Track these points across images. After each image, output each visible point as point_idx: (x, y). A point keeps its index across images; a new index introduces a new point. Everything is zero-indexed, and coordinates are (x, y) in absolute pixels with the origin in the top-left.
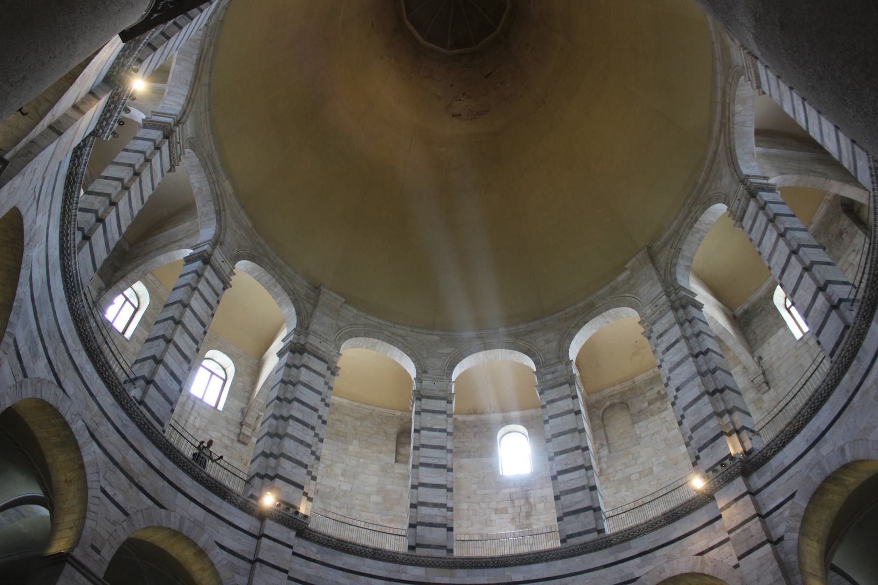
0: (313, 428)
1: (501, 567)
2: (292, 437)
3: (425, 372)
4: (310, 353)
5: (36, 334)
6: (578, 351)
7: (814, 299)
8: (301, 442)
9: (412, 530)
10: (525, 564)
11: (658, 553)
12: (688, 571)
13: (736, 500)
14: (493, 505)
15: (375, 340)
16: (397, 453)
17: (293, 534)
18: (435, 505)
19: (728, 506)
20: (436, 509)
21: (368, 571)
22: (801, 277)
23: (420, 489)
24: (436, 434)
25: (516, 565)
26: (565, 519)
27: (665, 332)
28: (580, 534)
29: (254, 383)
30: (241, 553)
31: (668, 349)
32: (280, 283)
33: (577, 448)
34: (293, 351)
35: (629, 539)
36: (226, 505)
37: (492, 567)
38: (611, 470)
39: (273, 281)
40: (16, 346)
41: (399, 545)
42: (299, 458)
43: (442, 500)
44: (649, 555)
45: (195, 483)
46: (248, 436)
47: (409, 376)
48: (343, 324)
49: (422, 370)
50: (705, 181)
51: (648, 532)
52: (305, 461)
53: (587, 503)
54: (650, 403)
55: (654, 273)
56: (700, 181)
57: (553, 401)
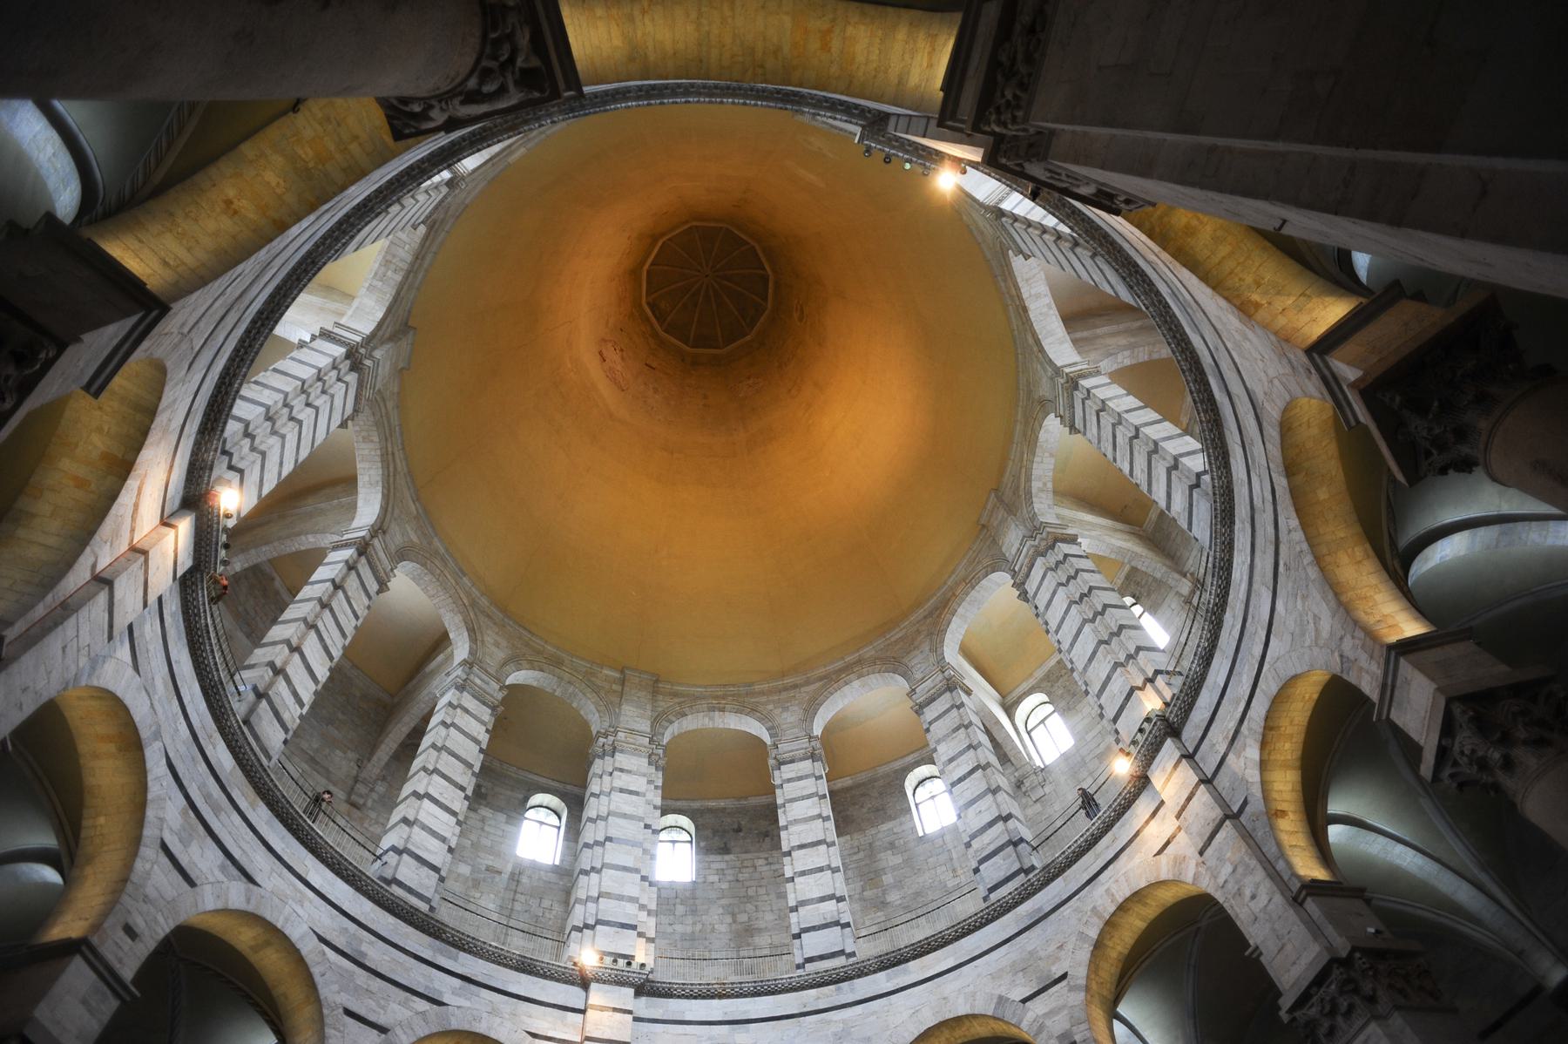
7: (823, 899)
8: (281, 464)
10: (333, 870)
11: (485, 993)
13: (615, 1010)
15: (376, 439)
18: (295, 694)
19: (602, 1009)
21: (186, 701)
22: (821, 869)
24: (349, 611)
25: (323, 861)
27: (629, 772)
28: (410, 890)
31: (622, 791)
38: (373, 815)
39: (405, 266)
44: (473, 987)
49: (378, 529)
50: (762, 693)
51: (488, 960)
55: (649, 707)
56: (757, 688)
57: (466, 711)
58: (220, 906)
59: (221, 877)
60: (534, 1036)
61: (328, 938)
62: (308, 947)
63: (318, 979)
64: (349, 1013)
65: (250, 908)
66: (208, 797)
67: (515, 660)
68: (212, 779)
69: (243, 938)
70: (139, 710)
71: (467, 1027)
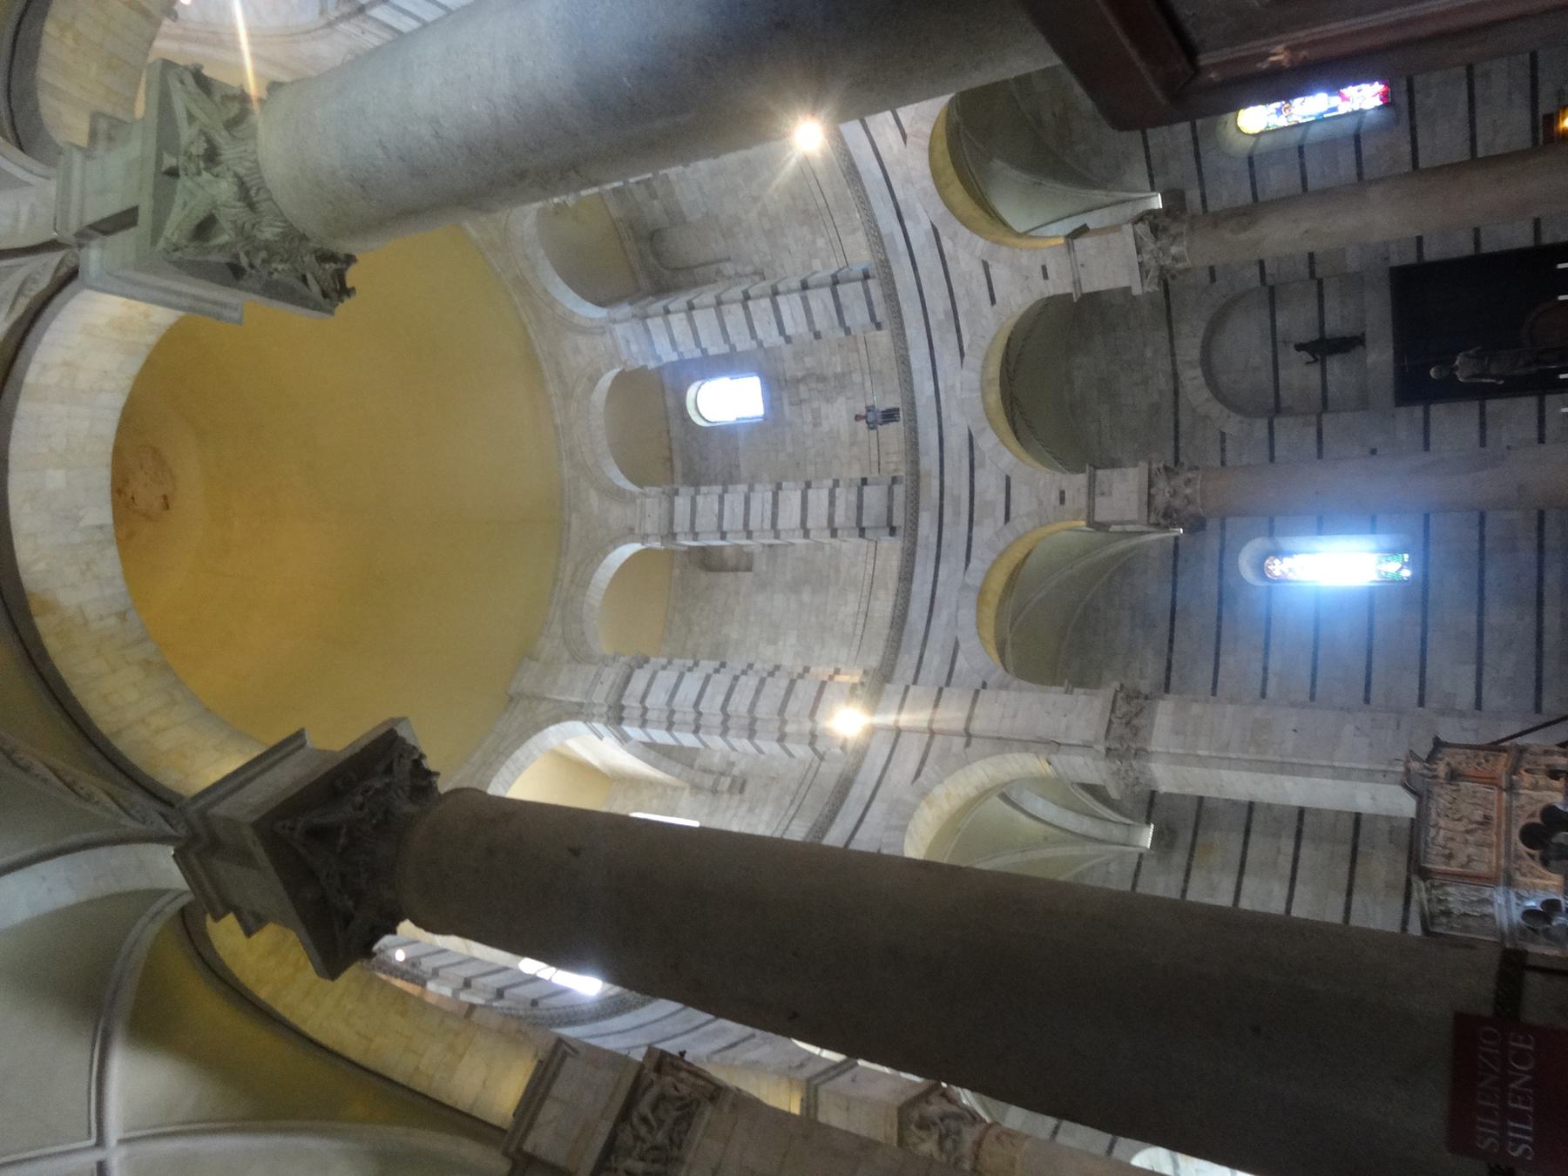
0: (736, 678)
2: (753, 705)
3: (631, 530)
4: (621, 696)
5: (694, 1034)
6: (589, 304)
8: (758, 692)
9: (868, 533)
11: (899, 195)
12: (926, 155)
14: (807, 429)
16: (736, 569)
17: (888, 686)
20: (838, 502)
21: (930, 587)
23: (810, 525)
26: (848, 323)
28: (870, 304)
29: (651, 783)
30: (923, 748)
32: (512, 753)
33: (746, 308)
34: (620, 720)
35: (879, 237)
36: (861, 777)
38: (756, 259)
39: (509, 763)
40: (719, 1051)
41: (891, 549)
42: (783, 692)
43: (824, 494)
44: (902, 208)
45: (838, 820)
46: (733, 781)
47: (636, 557)
48: (566, 656)
49: (629, 534)
51: (871, 209)
52: (784, 683)
53: (826, 293)
54: (655, 197)
58: (1003, 448)
59: (988, 461)
60: (904, 137)
64: (993, 300)
65: (987, 424)
66: (957, 514)
67: (568, 324)
68: (946, 520)
70: (967, 615)
71: (938, 197)
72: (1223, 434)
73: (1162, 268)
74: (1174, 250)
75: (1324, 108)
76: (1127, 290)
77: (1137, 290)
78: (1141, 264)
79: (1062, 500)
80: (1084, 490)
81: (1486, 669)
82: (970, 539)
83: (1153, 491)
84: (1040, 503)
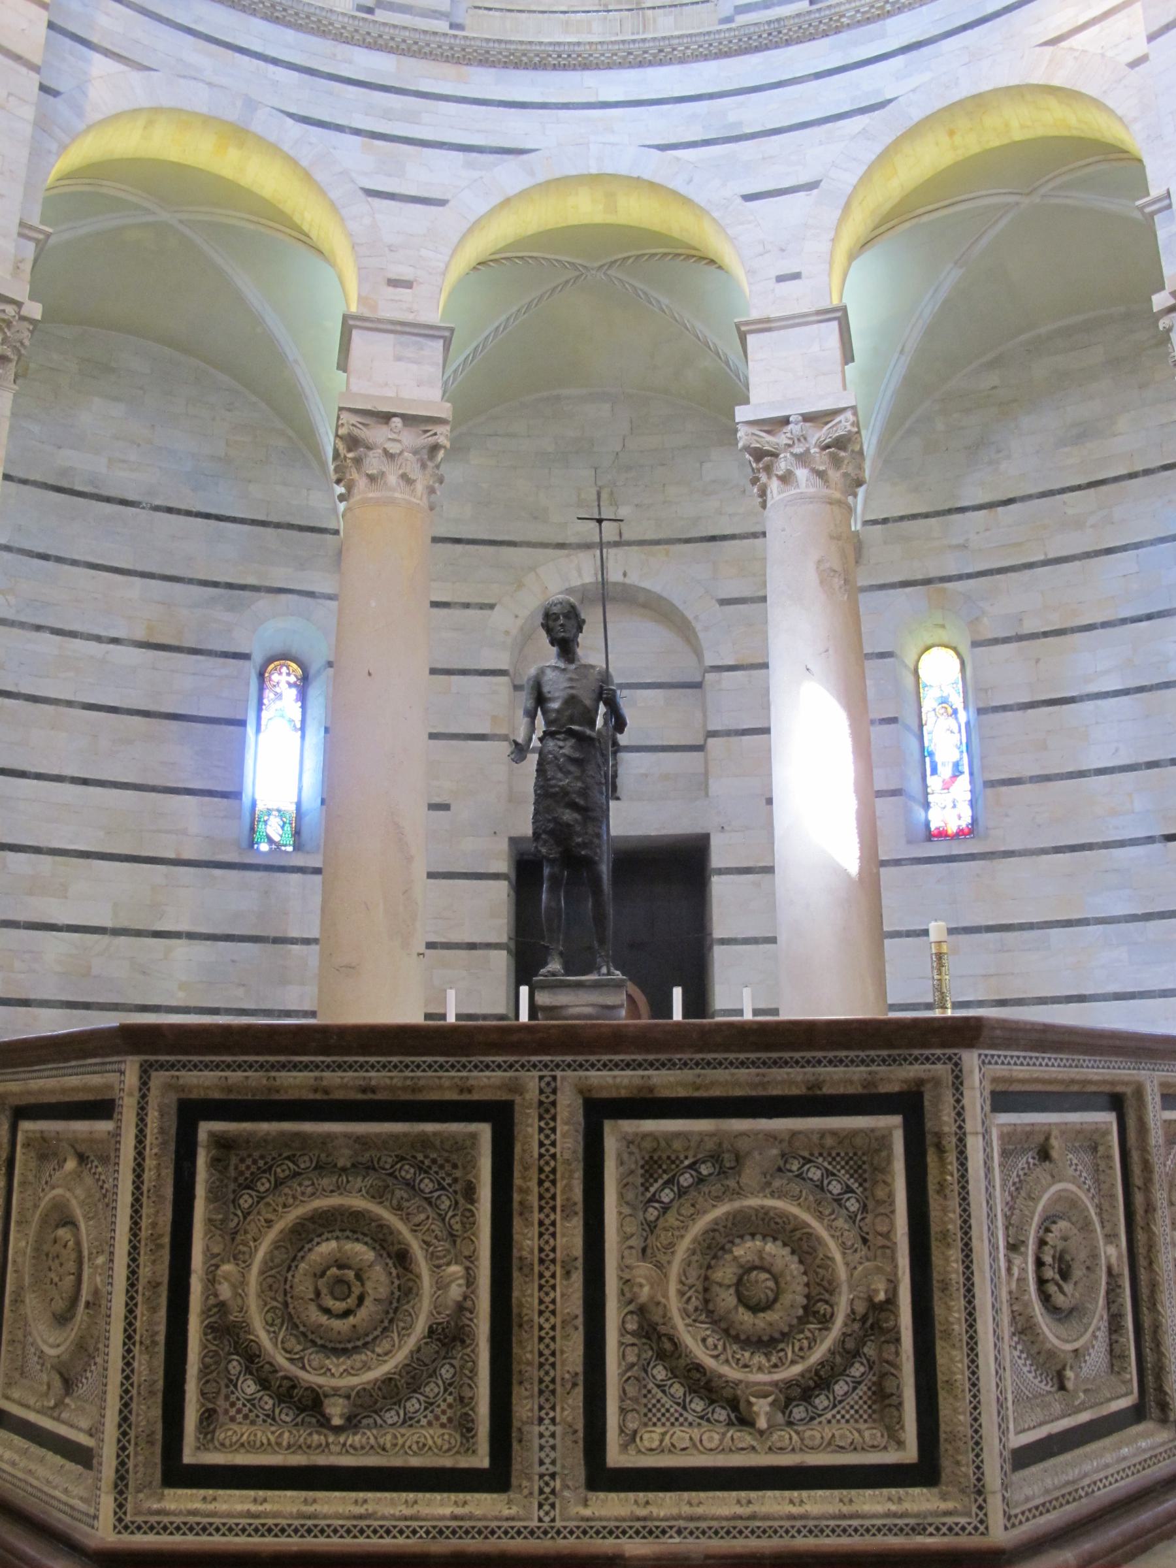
1: (574, 68)
10: (631, 66)
37: (555, 67)
61: (673, 140)
62: (654, 167)
63: (683, 190)
64: (748, 198)
65: (541, 179)
66: (387, 114)
69: (585, 209)
70: (199, 99)
72: (491, 607)
73: (775, 455)
74: (802, 474)
75: (937, 758)
76: (746, 401)
77: (742, 414)
78: (785, 421)
79: (394, 283)
80: (409, 317)
81: (105, 940)
82: (339, 128)
83: (397, 421)
84: (391, 248)
